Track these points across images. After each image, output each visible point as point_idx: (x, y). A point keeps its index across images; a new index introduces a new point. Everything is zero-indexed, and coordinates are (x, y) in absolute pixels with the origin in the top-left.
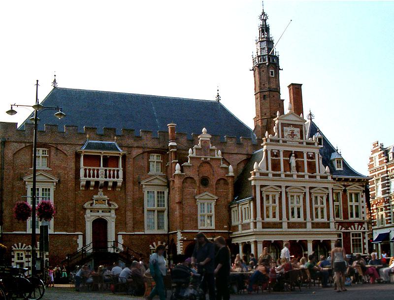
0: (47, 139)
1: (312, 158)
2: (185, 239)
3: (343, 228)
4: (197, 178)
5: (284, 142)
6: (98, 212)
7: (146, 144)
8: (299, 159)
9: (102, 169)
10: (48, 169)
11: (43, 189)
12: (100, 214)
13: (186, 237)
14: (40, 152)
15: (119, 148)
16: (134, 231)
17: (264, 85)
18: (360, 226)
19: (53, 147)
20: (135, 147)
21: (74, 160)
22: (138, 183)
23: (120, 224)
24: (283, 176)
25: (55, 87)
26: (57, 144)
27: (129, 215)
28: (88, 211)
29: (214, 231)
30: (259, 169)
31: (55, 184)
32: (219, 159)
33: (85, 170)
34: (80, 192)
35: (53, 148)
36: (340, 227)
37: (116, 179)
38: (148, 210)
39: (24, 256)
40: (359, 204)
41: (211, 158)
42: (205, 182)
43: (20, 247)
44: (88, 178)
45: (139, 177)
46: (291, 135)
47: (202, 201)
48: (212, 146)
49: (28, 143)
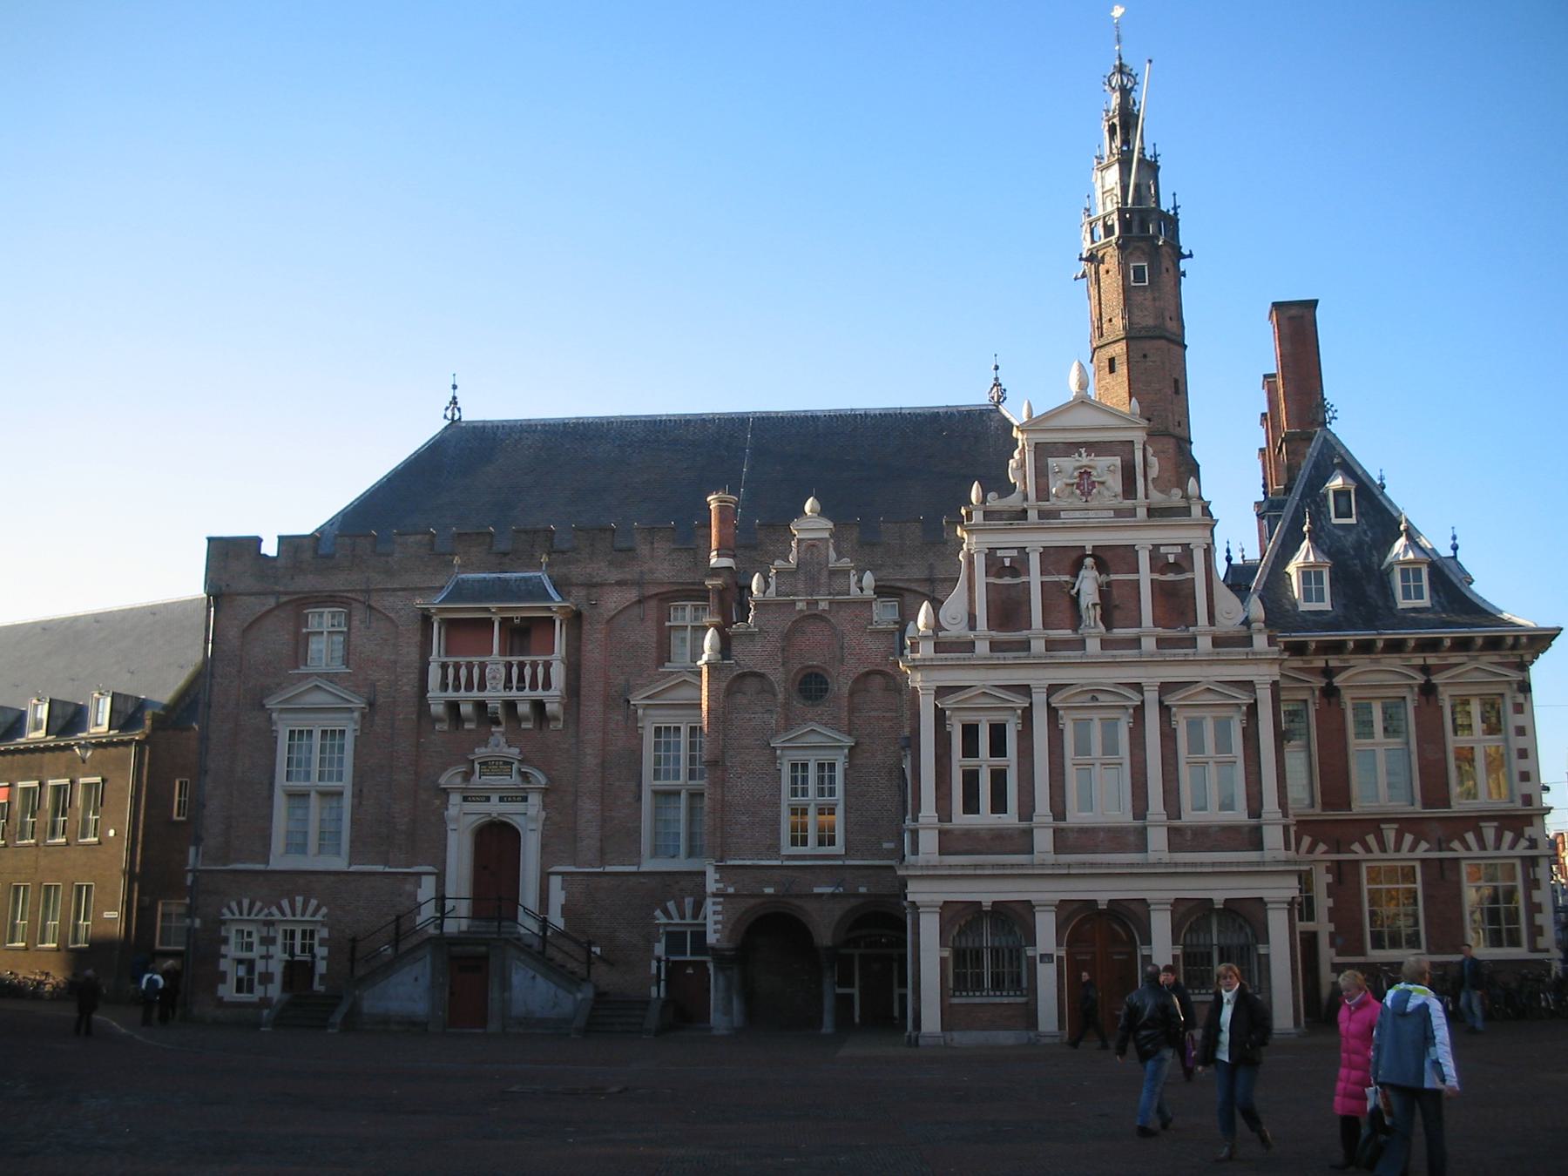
0: (337, 582)
1: (1177, 567)
2: (731, 890)
3: (1424, 845)
4: (776, 675)
5: (1043, 514)
6: (488, 799)
7: (651, 571)
8: (1113, 577)
9: (496, 661)
10: (343, 669)
11: (324, 732)
12: (495, 808)
13: (733, 884)
14: (323, 620)
15: (551, 591)
16: (602, 864)
17: (1110, 320)
18: (1508, 836)
19: (360, 602)
20: (611, 584)
21: (418, 638)
22: (620, 701)
23: (558, 839)
24: (1038, 646)
26: (368, 591)
27: (589, 808)
28: (455, 799)
29: (840, 863)
30: (937, 626)
31: (356, 715)
32: (868, 603)
33: (444, 667)
34: (433, 737)
35: (358, 605)
36: (1408, 839)
37: (539, 693)
38: (656, 793)
39: (255, 939)
40: (1506, 740)
41: (831, 602)
42: (812, 686)
43: (245, 911)
44: (451, 694)
45: (627, 681)
46: (1078, 486)
48: (838, 559)
49: (286, 593)
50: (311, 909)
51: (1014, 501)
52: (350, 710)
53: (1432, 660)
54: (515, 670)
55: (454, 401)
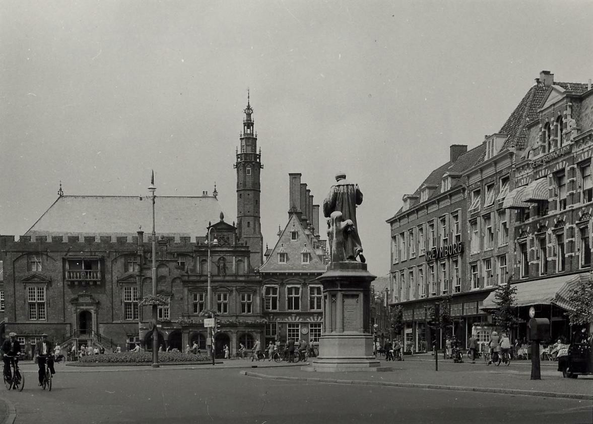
2: (145, 328)
3: (301, 319)
12: (84, 308)
18: (320, 318)
25: (61, 195)
36: (298, 318)
37: (95, 279)
44: (72, 279)
52: (45, 283)
55: (61, 190)
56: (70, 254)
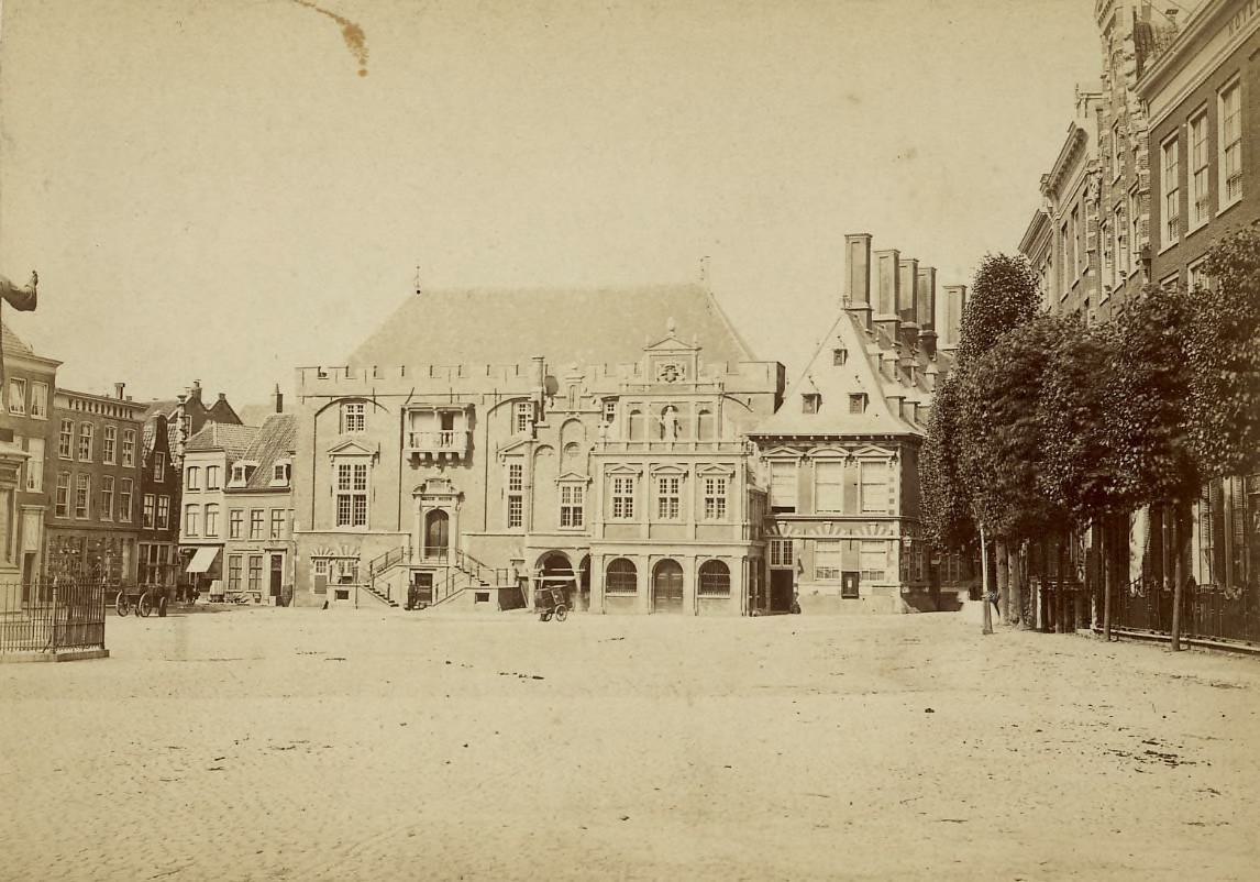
4: (557, 451)
12: (436, 503)
28: (418, 499)
33: (412, 435)
36: (836, 529)
44: (415, 449)
47: (567, 485)
50: (351, 552)
51: (639, 381)
53: (854, 445)
54: (445, 437)
56: (413, 399)
